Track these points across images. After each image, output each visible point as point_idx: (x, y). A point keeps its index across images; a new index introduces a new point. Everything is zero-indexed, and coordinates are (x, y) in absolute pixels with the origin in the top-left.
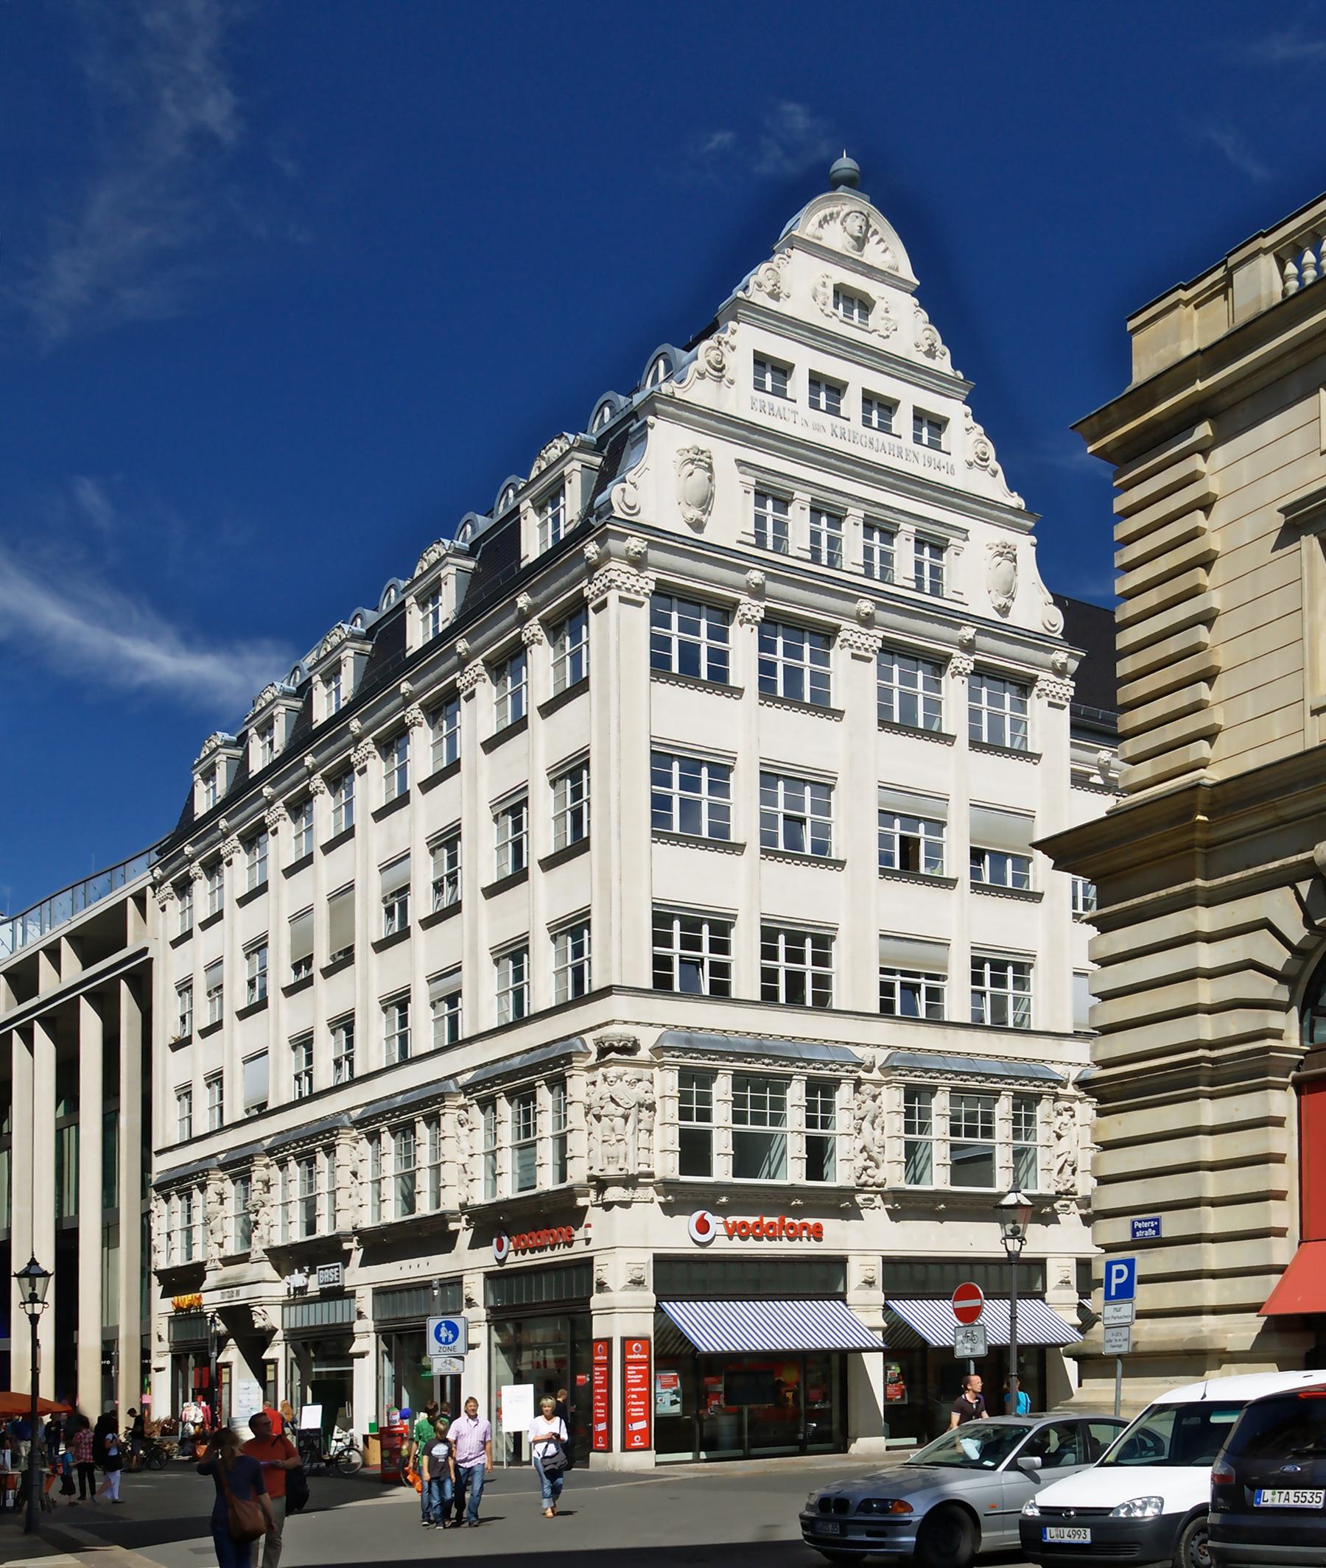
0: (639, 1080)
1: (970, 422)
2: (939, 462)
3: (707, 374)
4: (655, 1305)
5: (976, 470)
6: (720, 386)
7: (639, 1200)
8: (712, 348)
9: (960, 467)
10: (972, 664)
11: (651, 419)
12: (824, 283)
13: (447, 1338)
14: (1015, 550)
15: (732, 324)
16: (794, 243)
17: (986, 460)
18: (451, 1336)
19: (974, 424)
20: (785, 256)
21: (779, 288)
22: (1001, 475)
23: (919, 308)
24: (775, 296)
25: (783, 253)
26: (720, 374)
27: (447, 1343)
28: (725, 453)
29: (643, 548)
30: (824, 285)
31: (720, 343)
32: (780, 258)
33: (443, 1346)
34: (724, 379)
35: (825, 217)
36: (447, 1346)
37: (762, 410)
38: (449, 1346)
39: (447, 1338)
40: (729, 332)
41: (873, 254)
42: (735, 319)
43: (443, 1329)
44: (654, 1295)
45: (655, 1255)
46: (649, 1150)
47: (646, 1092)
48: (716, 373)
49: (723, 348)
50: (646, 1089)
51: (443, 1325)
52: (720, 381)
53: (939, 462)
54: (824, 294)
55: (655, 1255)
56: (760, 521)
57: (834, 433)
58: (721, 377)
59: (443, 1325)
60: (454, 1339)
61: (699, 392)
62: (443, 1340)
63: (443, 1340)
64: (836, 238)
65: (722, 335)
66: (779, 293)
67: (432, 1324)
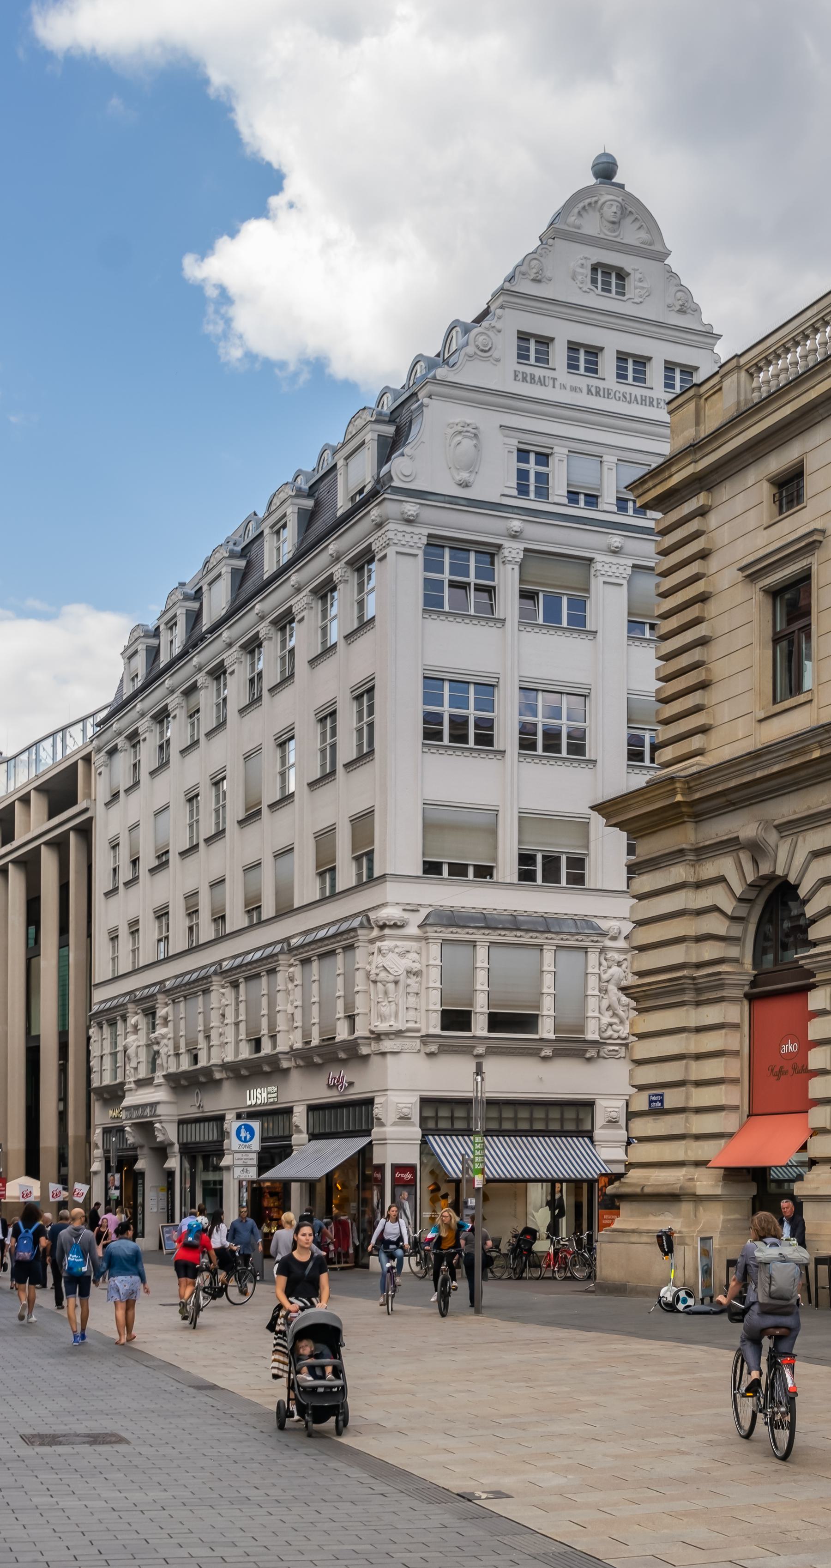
4: (420, 1137)
7: (408, 1051)
13: (246, 1137)
18: (248, 1137)
27: (245, 1141)
33: (242, 1143)
36: (245, 1144)
38: (247, 1144)
39: (246, 1137)
43: (243, 1130)
44: (420, 1130)
46: (416, 1009)
47: (414, 962)
50: (414, 959)
60: (251, 1139)
62: (243, 1139)
63: (243, 1139)
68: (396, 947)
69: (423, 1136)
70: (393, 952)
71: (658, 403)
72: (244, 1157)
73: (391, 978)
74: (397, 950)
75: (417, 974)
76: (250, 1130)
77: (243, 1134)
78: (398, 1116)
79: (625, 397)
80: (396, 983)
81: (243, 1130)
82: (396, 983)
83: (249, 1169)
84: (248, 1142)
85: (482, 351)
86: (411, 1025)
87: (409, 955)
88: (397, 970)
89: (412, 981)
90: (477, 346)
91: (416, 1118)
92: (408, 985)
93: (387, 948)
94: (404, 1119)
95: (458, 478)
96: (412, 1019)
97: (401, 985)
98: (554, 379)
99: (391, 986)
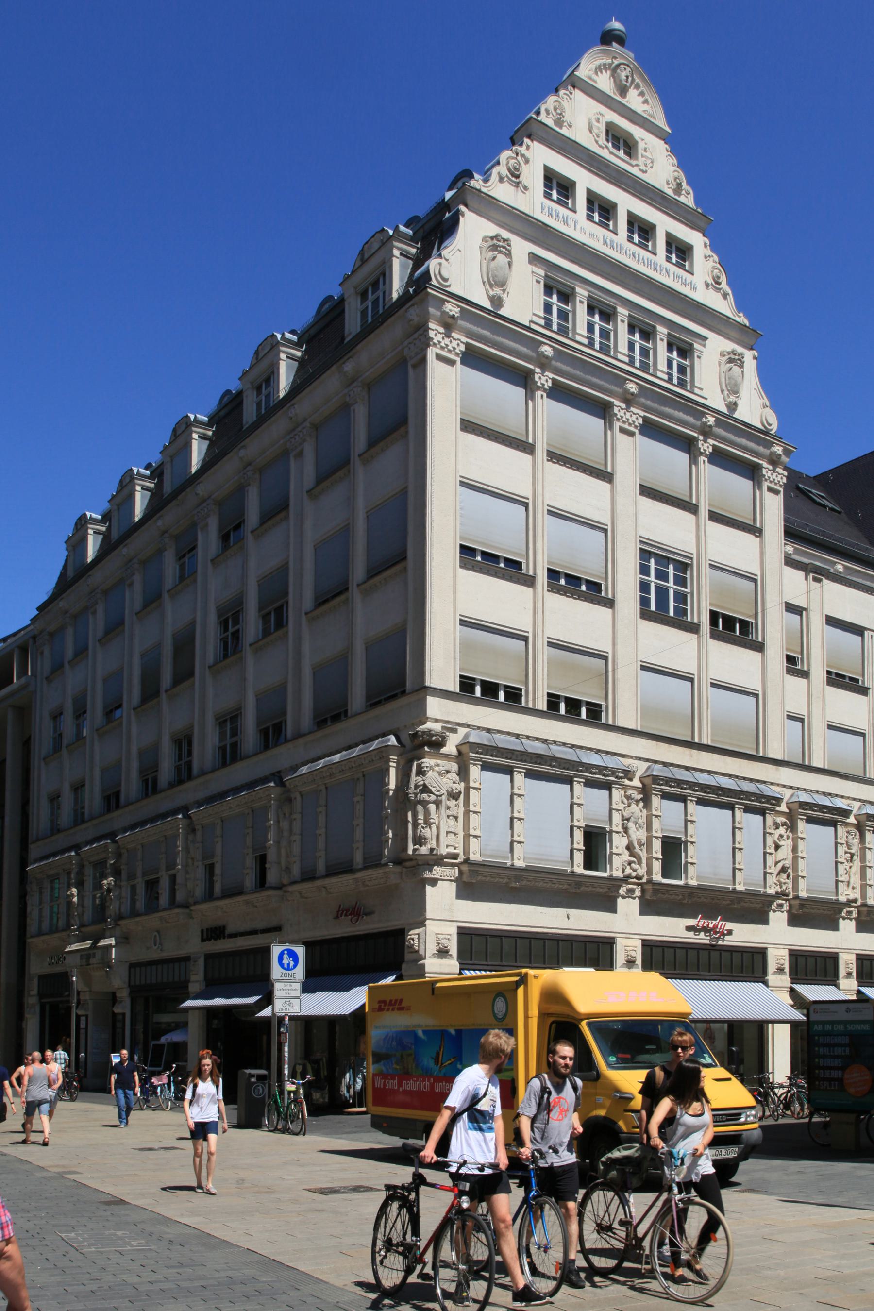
0: (448, 772)
1: (708, 252)
2: (685, 280)
3: (506, 179)
4: (458, 971)
5: (711, 291)
6: (517, 190)
7: (446, 878)
8: (513, 158)
9: (701, 286)
10: (711, 448)
11: (462, 208)
12: (599, 119)
13: (289, 965)
14: (743, 358)
15: (527, 141)
16: (575, 83)
17: (719, 284)
18: (292, 963)
19: (711, 253)
20: (568, 93)
21: (563, 117)
22: (731, 297)
23: (669, 153)
24: (559, 122)
25: (567, 90)
26: (518, 180)
27: (288, 969)
28: (521, 248)
29: (456, 313)
30: (598, 121)
31: (517, 154)
32: (565, 94)
33: (284, 971)
34: (520, 185)
35: (600, 66)
36: (288, 972)
37: (550, 215)
38: (290, 972)
39: (289, 965)
40: (524, 146)
41: (634, 100)
42: (529, 137)
43: (285, 956)
44: (457, 964)
45: (459, 928)
46: (456, 834)
47: (454, 783)
48: (514, 179)
49: (519, 158)
50: (454, 780)
51: (286, 952)
52: (517, 187)
53: (685, 280)
54: (598, 128)
55: (459, 928)
56: (548, 308)
57: (605, 242)
58: (518, 183)
59: (286, 952)
60: (295, 966)
61: (502, 192)
62: (286, 966)
63: (286, 966)
64: (605, 83)
65: (519, 148)
66: (563, 122)
67: (276, 950)
68: (438, 765)
69: (461, 969)
70: (433, 770)
71: (661, 270)
72: (287, 987)
73: (433, 798)
74: (437, 768)
75: (454, 796)
76: (293, 955)
77: (286, 961)
78: (438, 948)
79: (634, 256)
80: (438, 804)
81: (285, 956)
82: (438, 804)
83: (292, 1001)
84: (292, 969)
85: (513, 175)
86: (451, 850)
87: (449, 775)
88: (439, 789)
89: (452, 803)
90: (509, 170)
91: (454, 951)
92: (448, 808)
93: (428, 765)
94: (443, 953)
95: (491, 293)
96: (452, 844)
97: (443, 807)
98: (576, 223)
99: (432, 807)
